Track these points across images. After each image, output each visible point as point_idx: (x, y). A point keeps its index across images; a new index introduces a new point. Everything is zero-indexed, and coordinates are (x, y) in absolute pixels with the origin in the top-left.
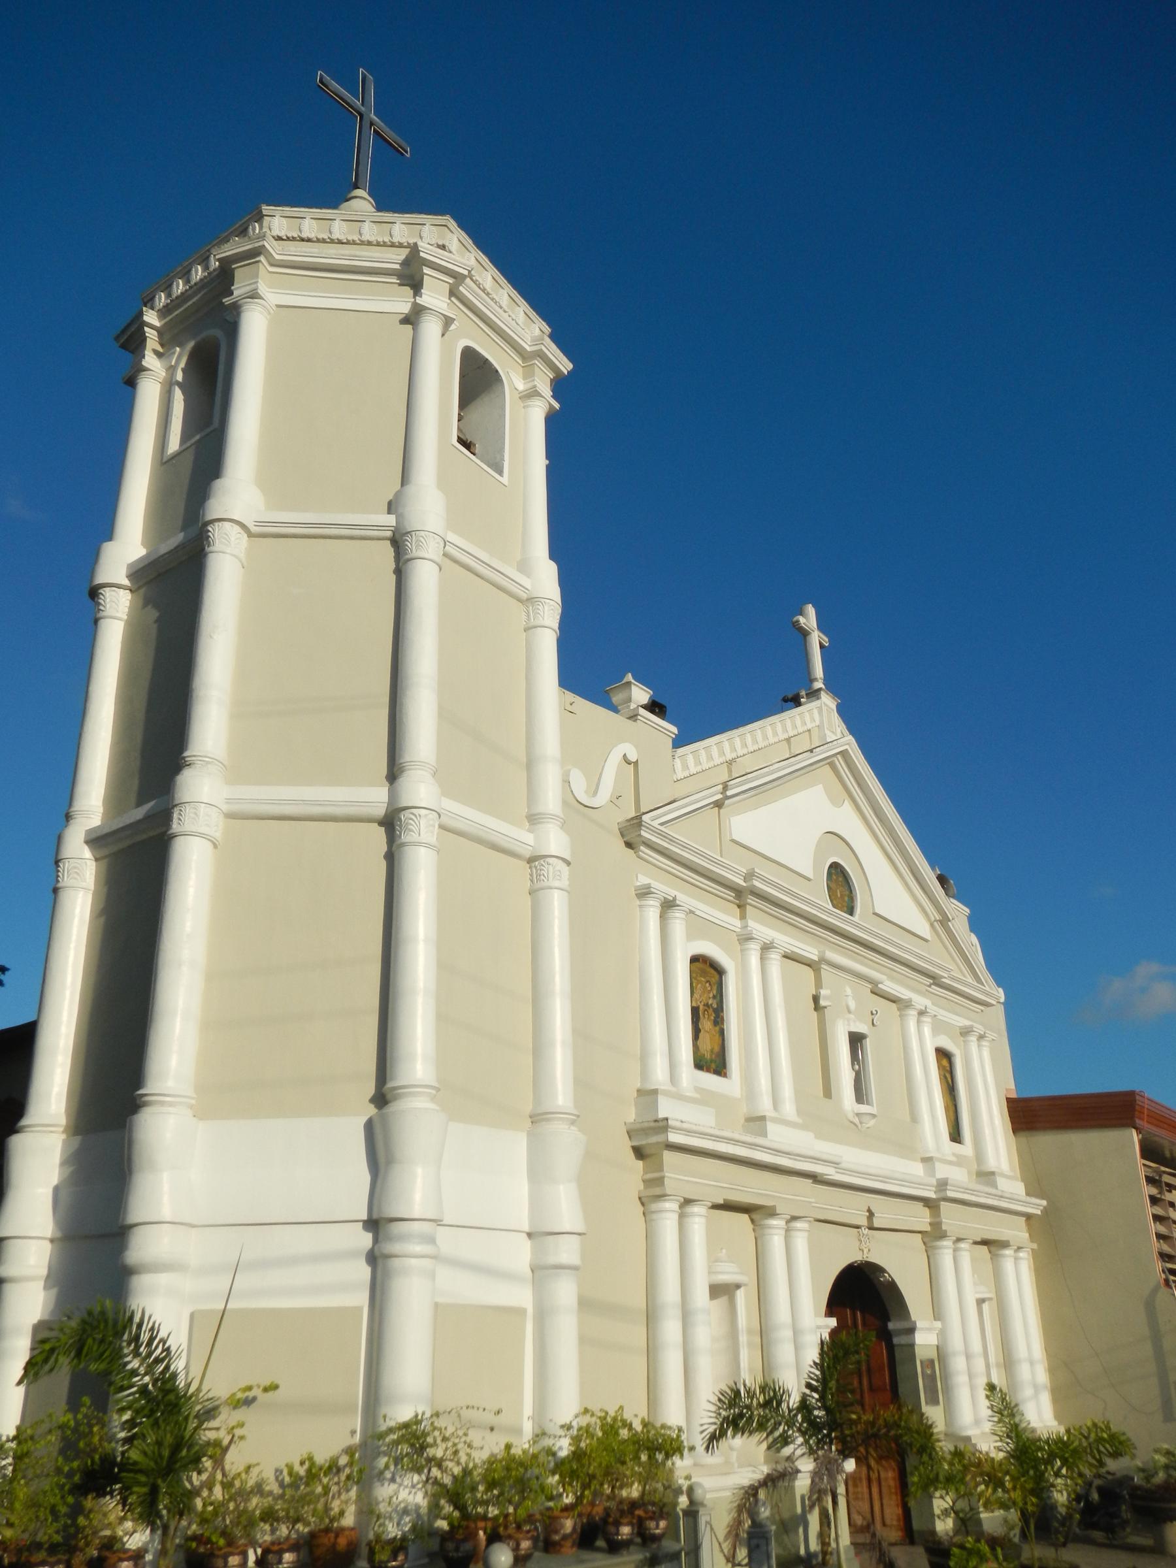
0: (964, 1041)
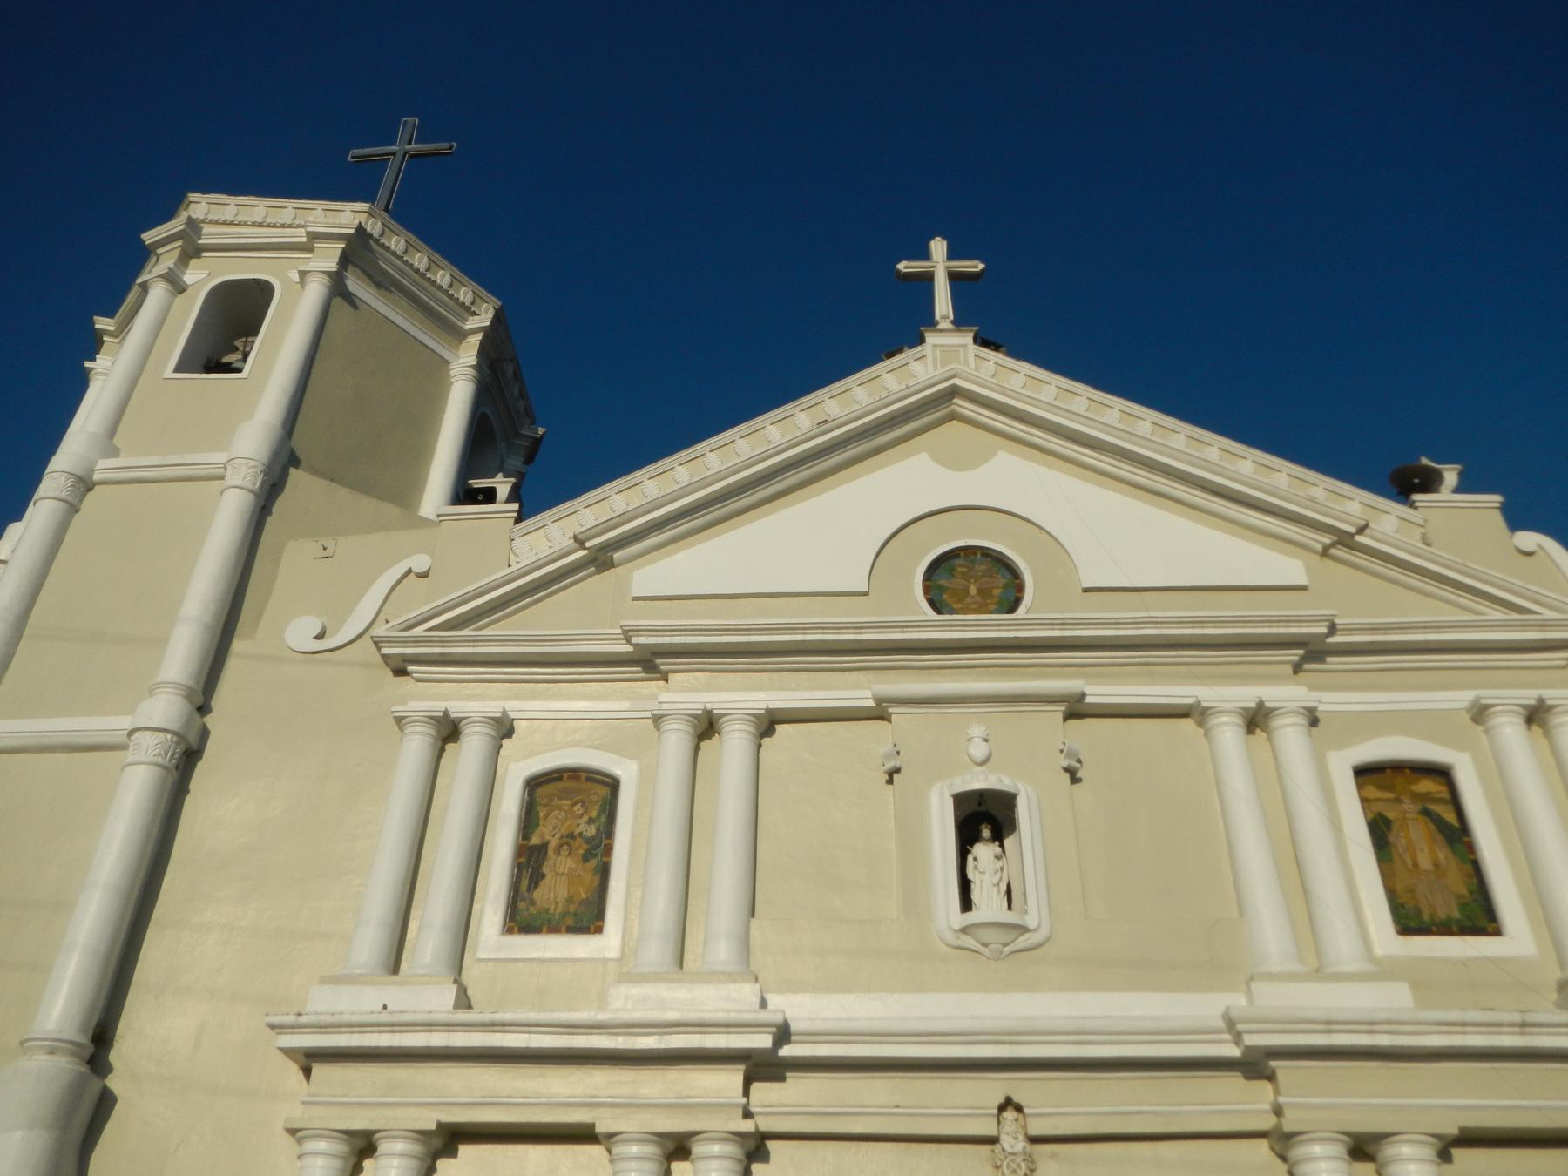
0: (1486, 732)
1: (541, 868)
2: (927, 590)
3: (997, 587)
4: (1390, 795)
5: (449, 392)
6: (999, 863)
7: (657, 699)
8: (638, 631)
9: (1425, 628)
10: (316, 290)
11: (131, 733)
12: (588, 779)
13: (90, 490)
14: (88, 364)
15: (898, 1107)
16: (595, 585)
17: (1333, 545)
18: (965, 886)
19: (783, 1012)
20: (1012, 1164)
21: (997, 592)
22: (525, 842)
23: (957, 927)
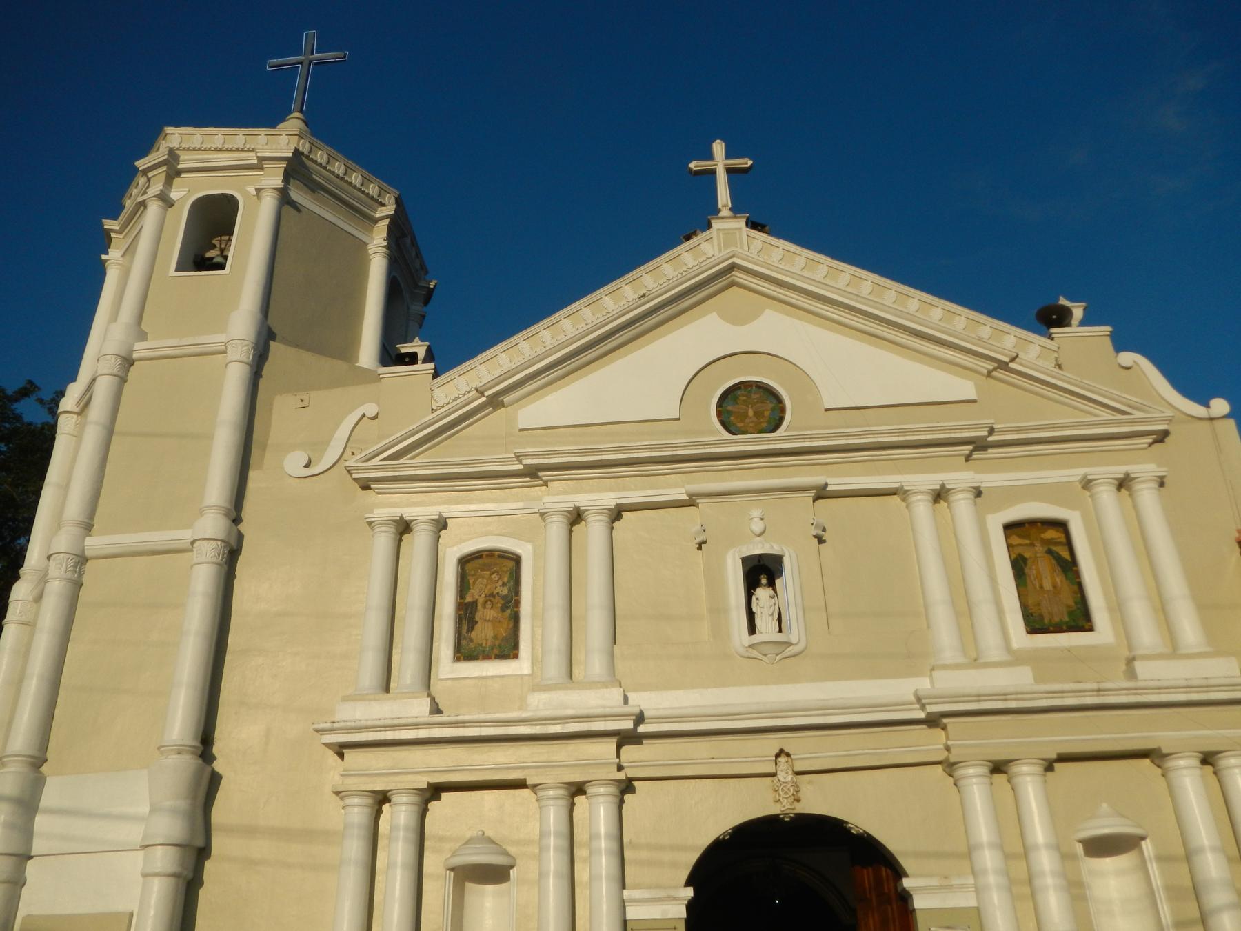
0: (1091, 496)
1: (474, 617)
2: (719, 414)
3: (767, 410)
4: (1027, 542)
5: (369, 266)
6: (773, 601)
7: (541, 500)
8: (526, 455)
9: (1054, 427)
10: (268, 204)
11: (193, 543)
12: (500, 556)
13: (132, 364)
14: (104, 257)
15: (713, 758)
16: (495, 420)
17: (995, 369)
18: (751, 616)
19: (639, 706)
20: (784, 788)
21: (767, 413)
22: (462, 601)
23: (747, 645)
